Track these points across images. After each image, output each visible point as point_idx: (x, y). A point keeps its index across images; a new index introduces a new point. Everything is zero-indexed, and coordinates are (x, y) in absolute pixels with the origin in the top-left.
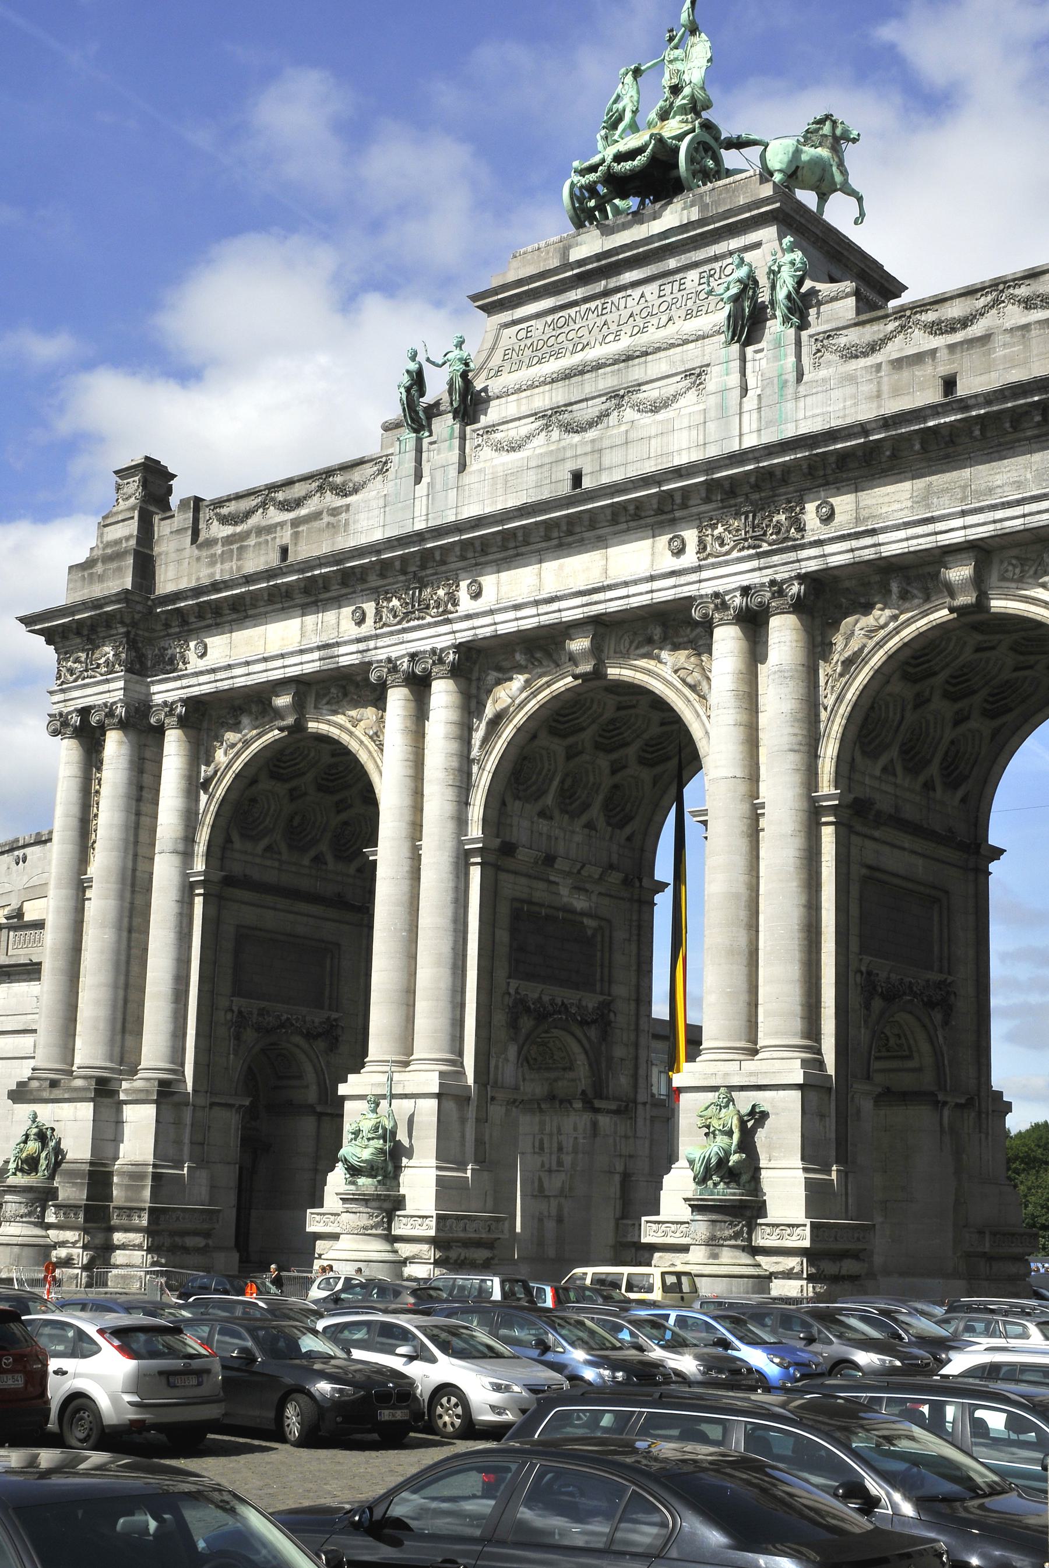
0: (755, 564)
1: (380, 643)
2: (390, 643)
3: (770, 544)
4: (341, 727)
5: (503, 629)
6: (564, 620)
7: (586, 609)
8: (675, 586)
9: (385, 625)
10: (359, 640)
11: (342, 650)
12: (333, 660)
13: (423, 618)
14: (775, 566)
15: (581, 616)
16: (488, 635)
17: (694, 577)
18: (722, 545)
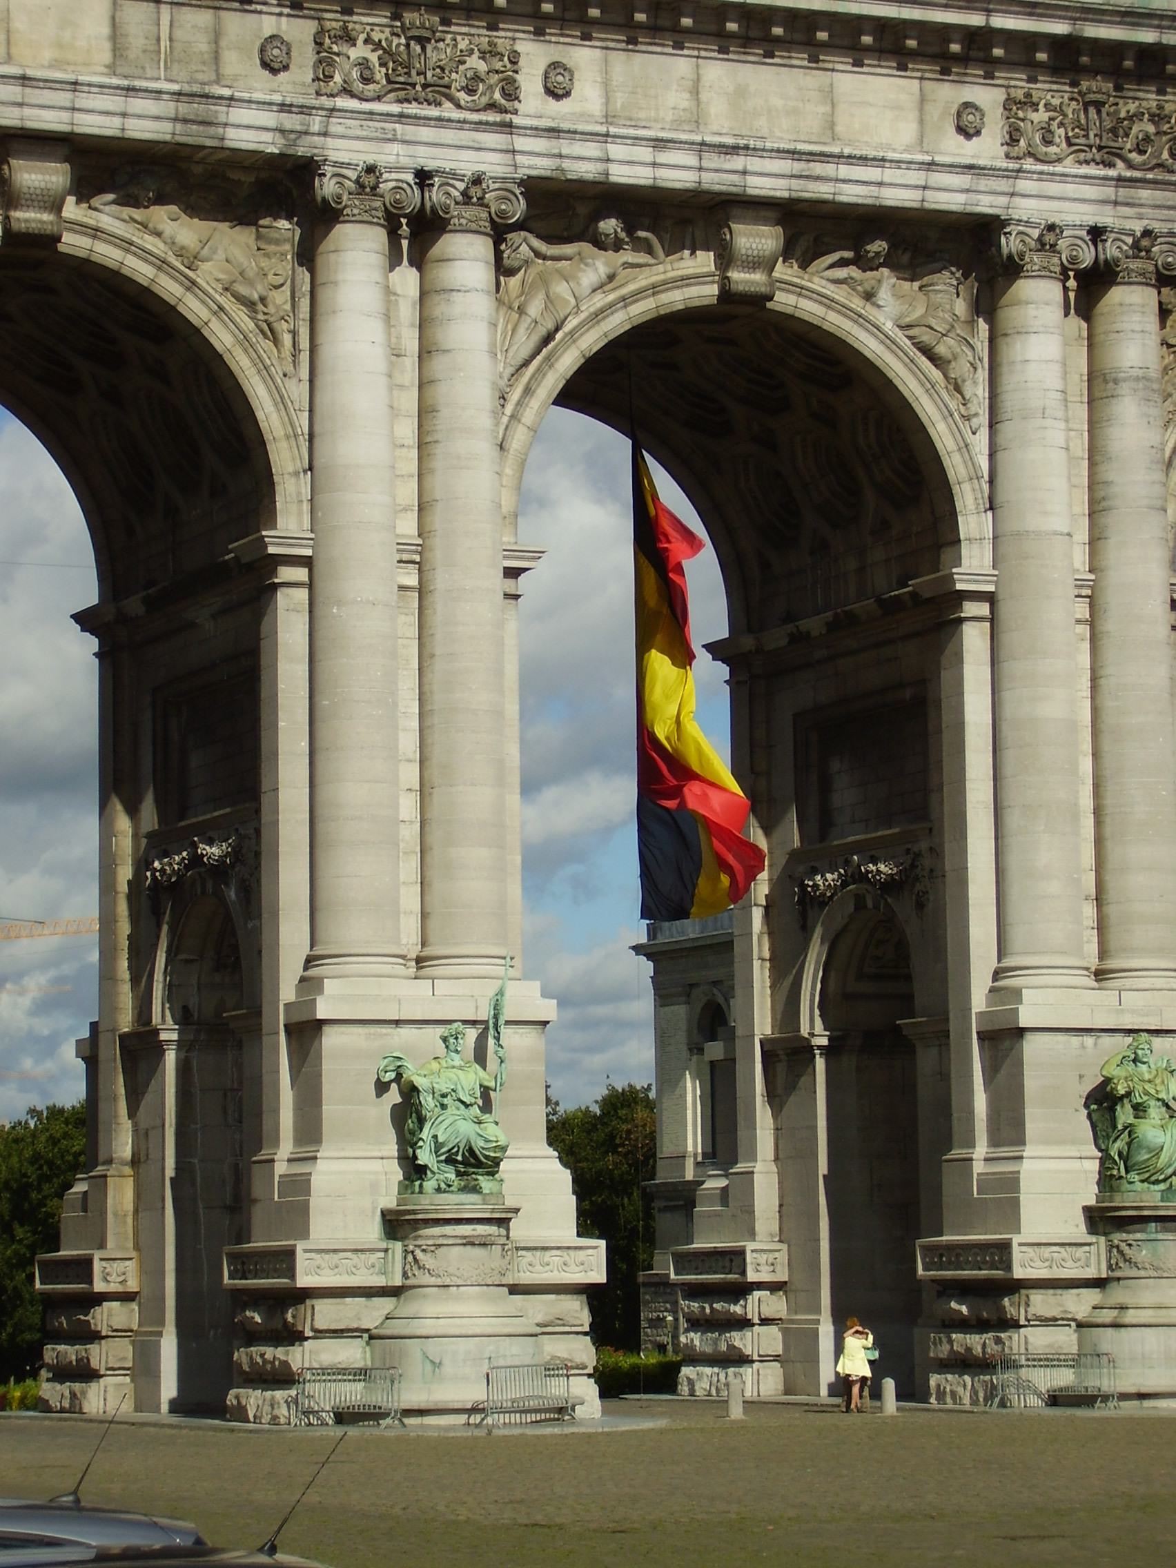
0: (1109, 192)
1: (336, 126)
2: (359, 132)
3: (1130, 165)
4: (162, 264)
5: (621, 175)
6: (750, 191)
7: (796, 184)
8: (967, 191)
9: (347, 91)
10: (284, 108)
11: (239, 115)
12: (212, 130)
13: (439, 104)
14: (1141, 205)
15: (786, 194)
16: (589, 177)
17: (1003, 185)
18: (1048, 142)
